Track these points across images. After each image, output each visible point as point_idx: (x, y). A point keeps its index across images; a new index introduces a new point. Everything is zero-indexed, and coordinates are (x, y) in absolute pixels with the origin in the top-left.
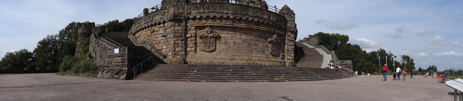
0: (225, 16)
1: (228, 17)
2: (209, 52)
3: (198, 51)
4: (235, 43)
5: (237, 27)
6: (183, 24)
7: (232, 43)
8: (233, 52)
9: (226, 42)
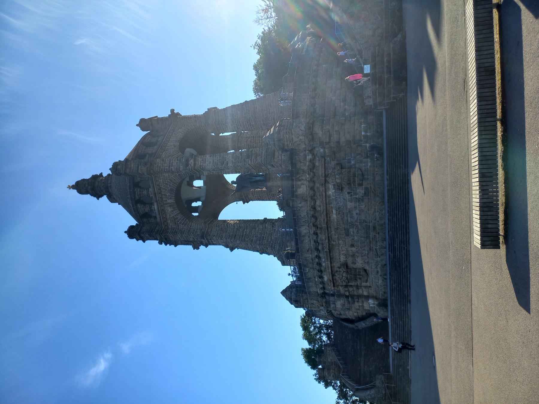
0: (317, 260)
1: (316, 256)
2: (367, 274)
3: (368, 284)
4: (352, 246)
5: (329, 244)
6: (332, 299)
7: (354, 249)
8: (366, 248)
9: (353, 256)
